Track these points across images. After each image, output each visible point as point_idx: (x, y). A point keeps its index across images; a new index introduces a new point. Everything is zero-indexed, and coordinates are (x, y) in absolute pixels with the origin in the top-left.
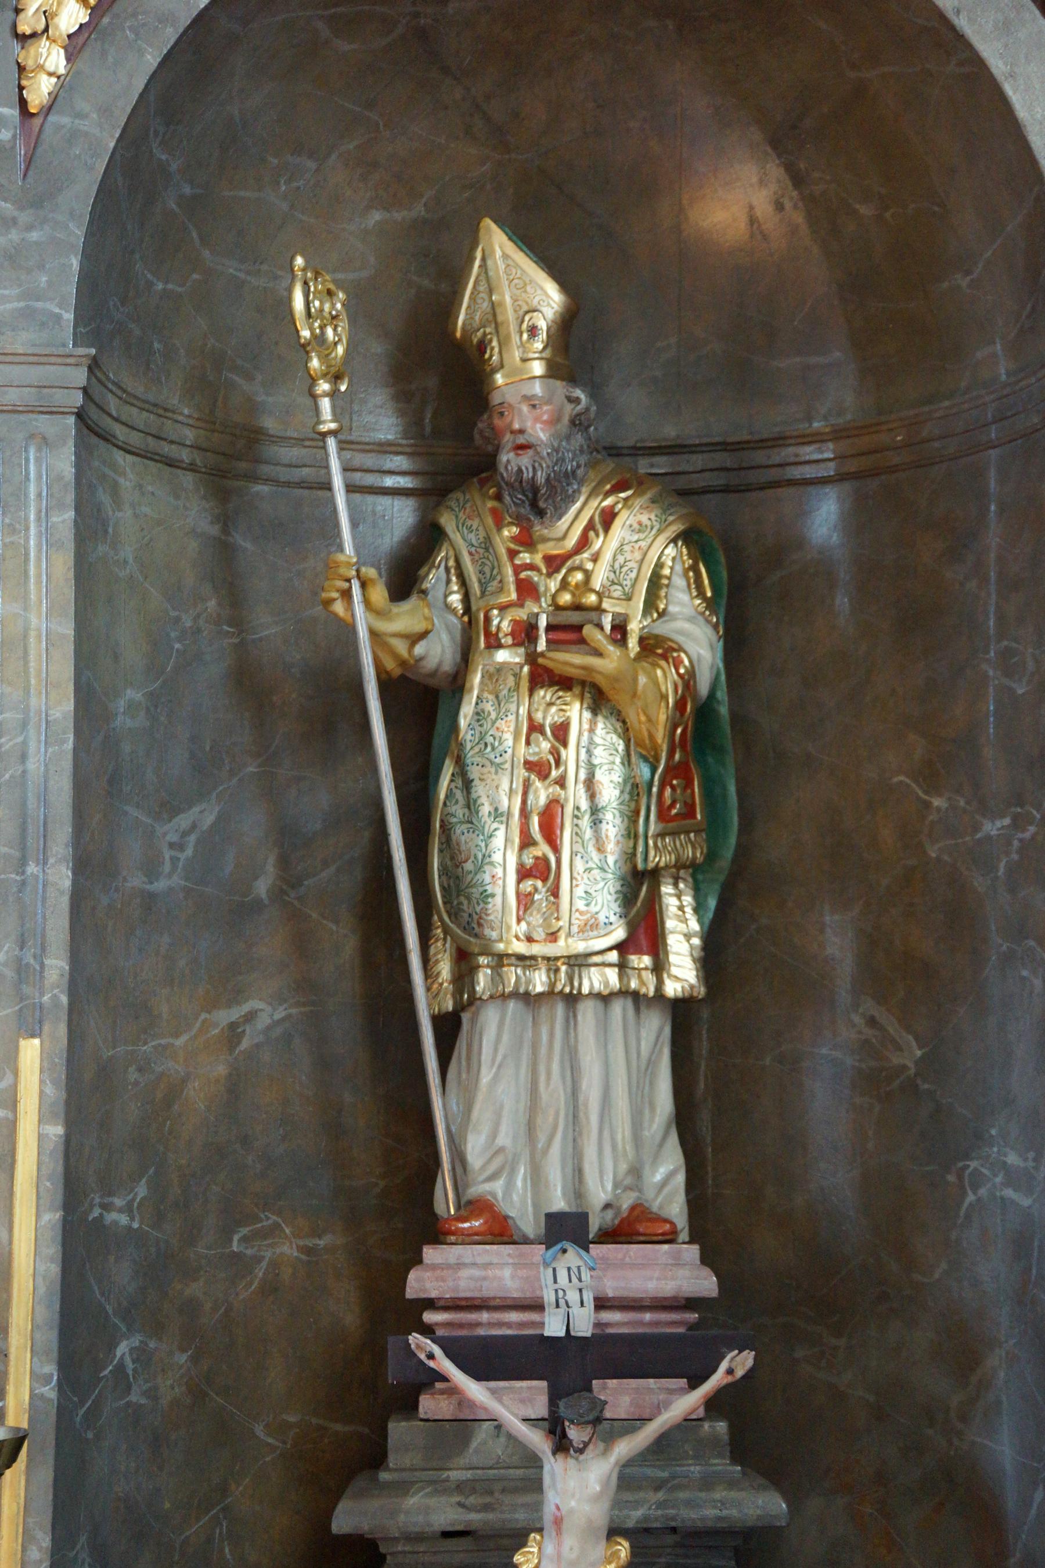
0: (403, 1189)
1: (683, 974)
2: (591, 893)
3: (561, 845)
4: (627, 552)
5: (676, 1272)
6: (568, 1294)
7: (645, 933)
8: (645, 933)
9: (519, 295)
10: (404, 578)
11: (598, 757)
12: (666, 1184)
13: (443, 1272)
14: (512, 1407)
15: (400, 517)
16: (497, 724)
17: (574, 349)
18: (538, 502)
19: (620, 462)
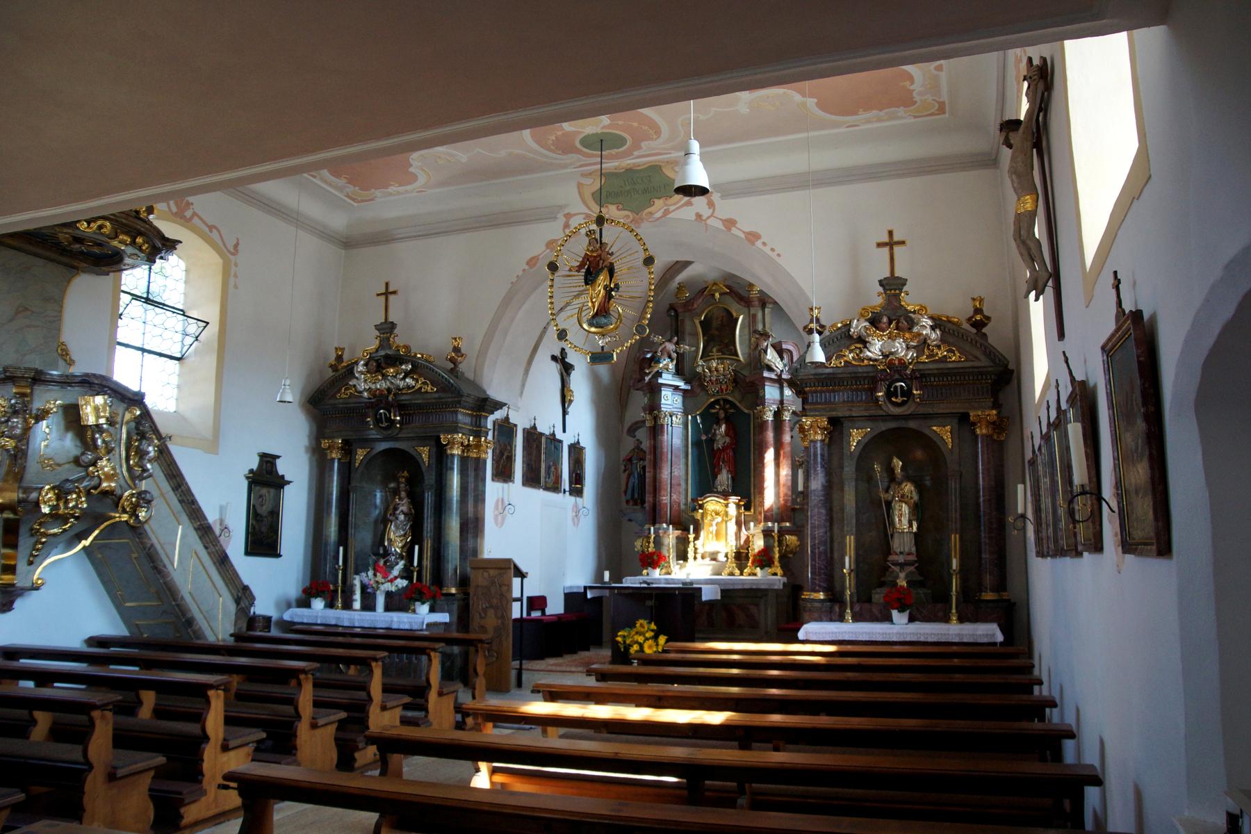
0: (888, 550)
1: (915, 529)
2: (905, 521)
3: (903, 519)
4: (908, 488)
5: (913, 558)
6: (901, 559)
7: (911, 525)
8: (911, 525)
9: (897, 463)
10: (887, 491)
11: (905, 508)
12: (914, 549)
13: (891, 558)
14: (897, 569)
15: (886, 484)
16: (896, 505)
17: (903, 468)
18: (900, 484)
19: (908, 478)
